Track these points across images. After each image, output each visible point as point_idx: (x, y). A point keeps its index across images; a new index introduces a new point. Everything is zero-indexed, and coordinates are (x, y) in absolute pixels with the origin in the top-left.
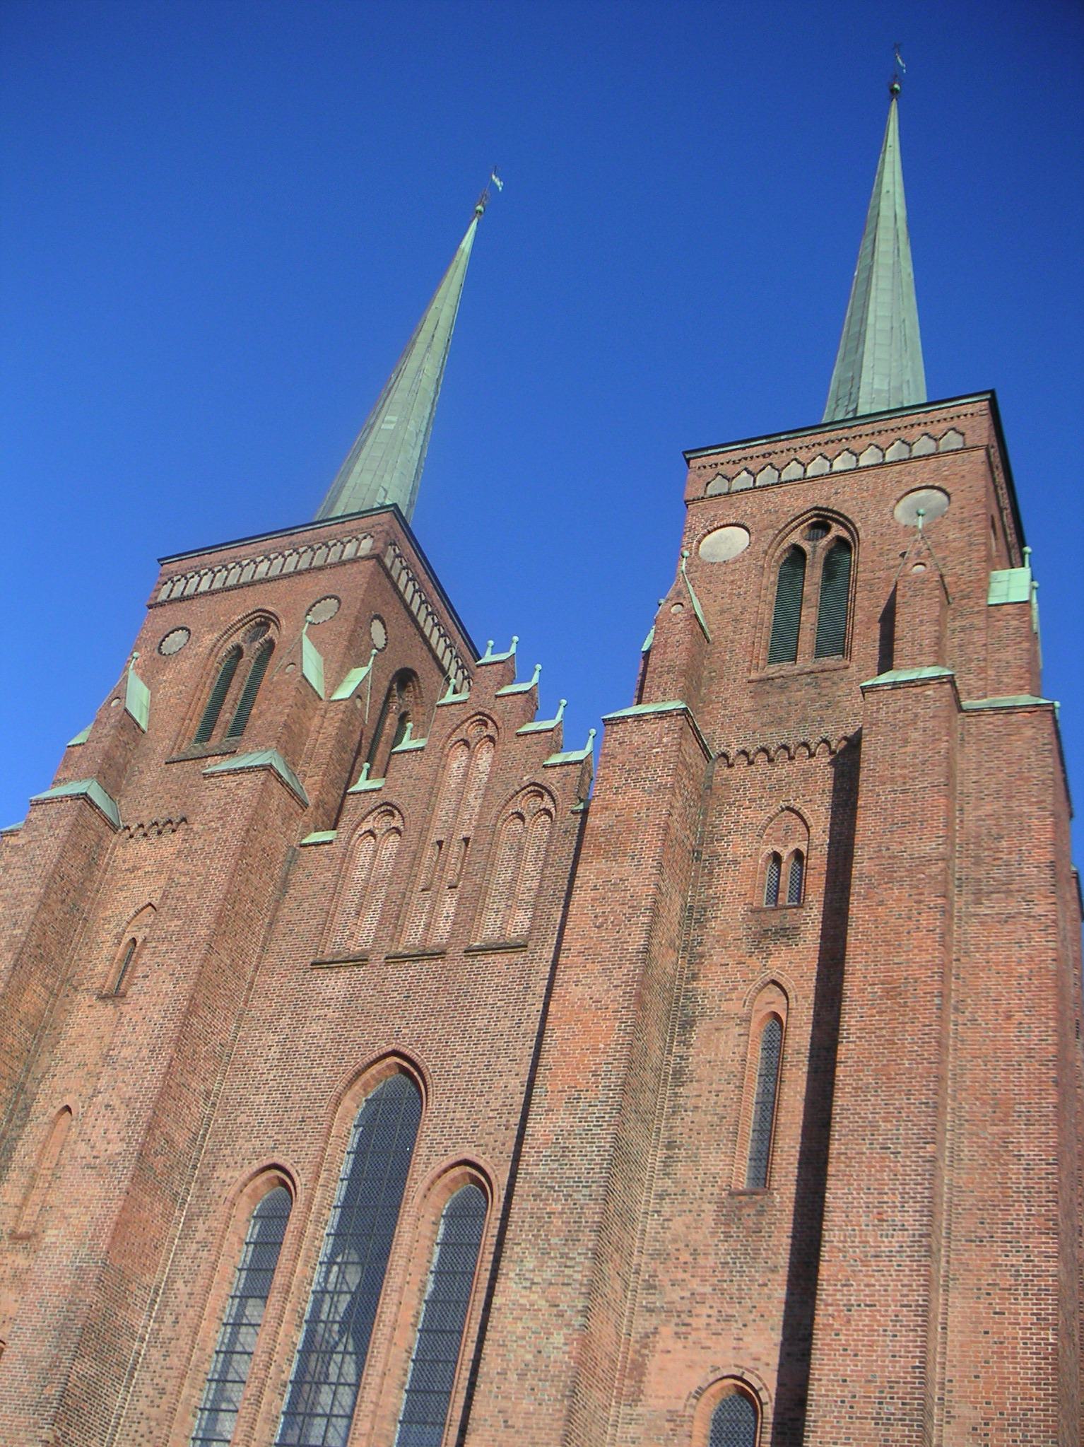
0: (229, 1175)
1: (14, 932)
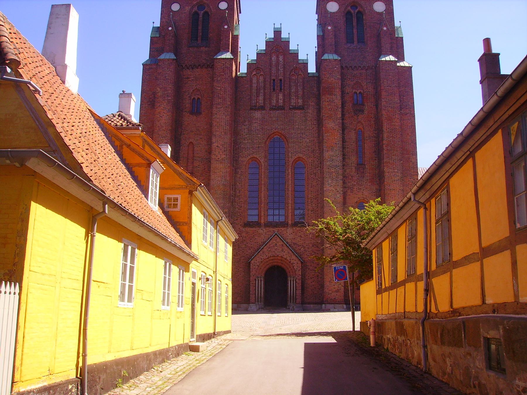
1: (169, 98)
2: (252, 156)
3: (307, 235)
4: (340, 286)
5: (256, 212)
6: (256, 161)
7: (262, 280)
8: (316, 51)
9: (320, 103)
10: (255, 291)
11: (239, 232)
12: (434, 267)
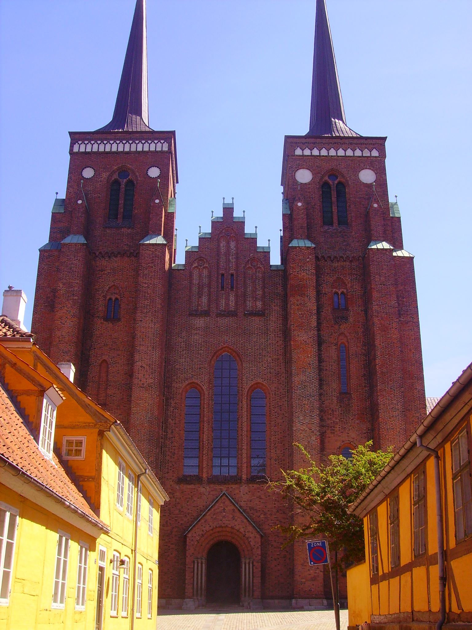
0: (178, 386)
2: (190, 382)
3: (269, 496)
4: (317, 572)
5: (195, 462)
6: (196, 388)
7: (204, 562)
8: (281, 236)
9: (287, 307)
10: (193, 580)
11: (171, 491)
12: (452, 544)
